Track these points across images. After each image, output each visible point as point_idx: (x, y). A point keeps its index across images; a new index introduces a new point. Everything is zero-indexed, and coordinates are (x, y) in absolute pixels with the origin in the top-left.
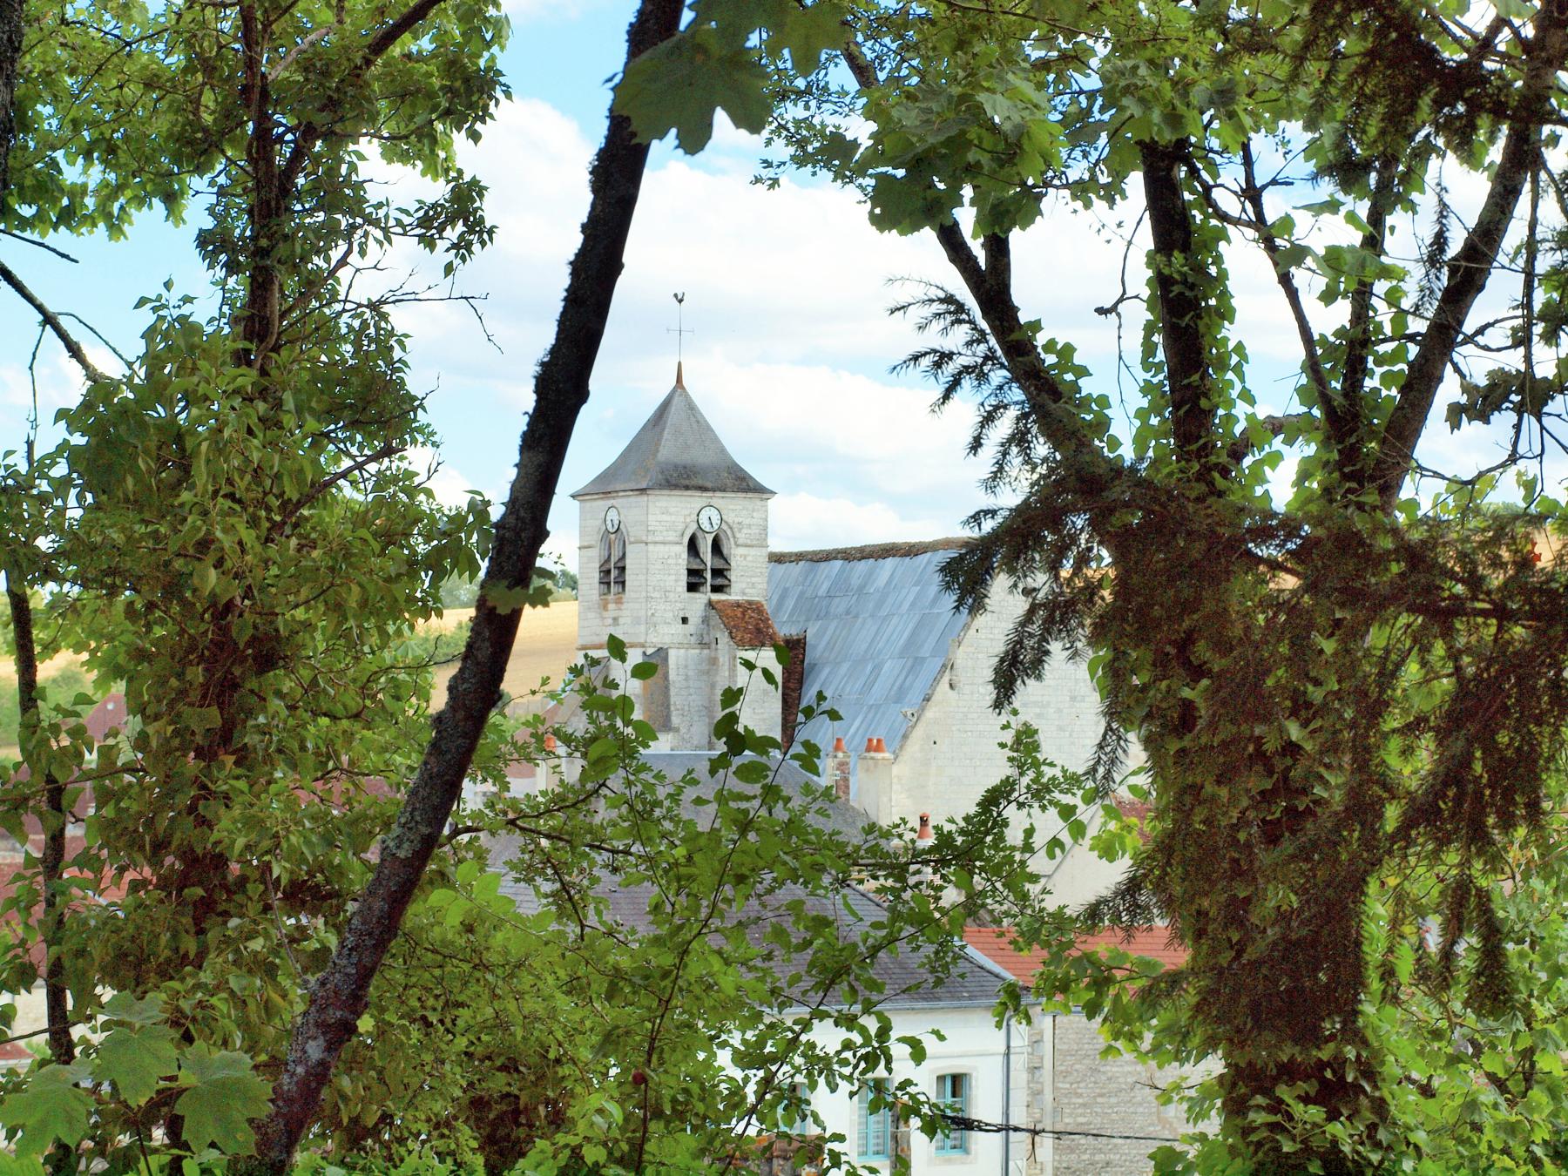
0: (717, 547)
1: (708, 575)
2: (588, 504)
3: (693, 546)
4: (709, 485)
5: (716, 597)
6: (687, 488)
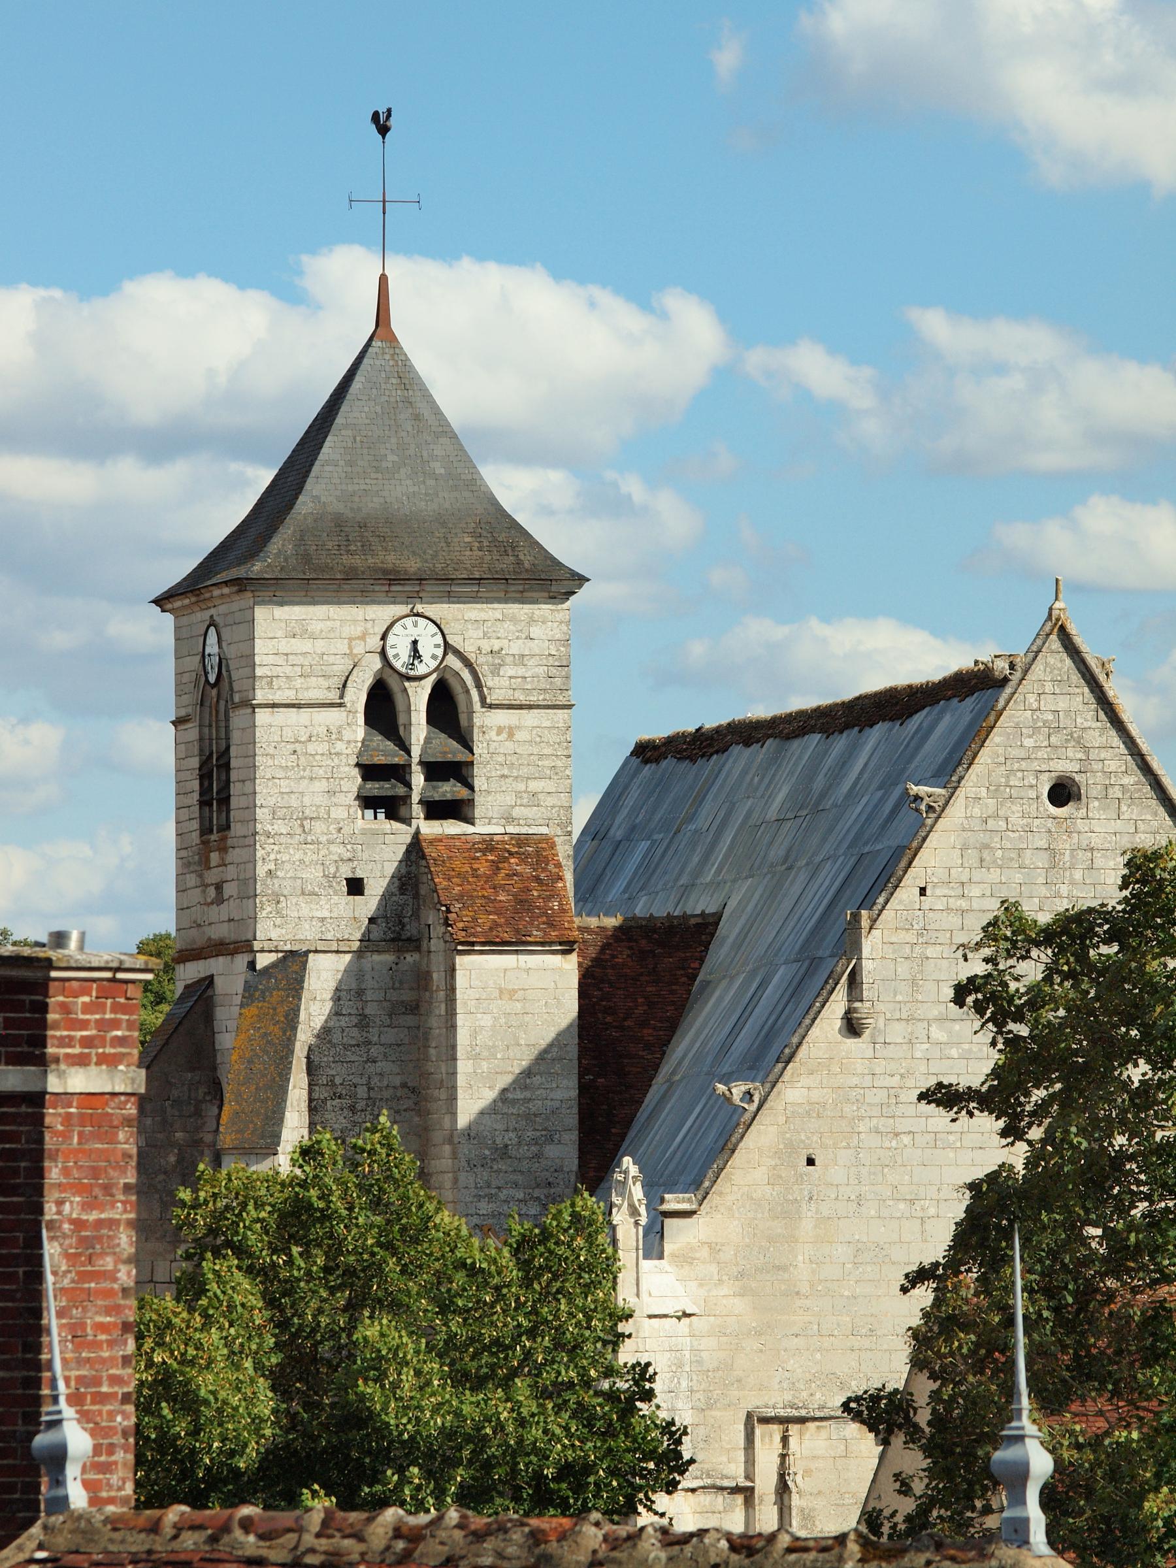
1: (418, 779)
2: (185, 620)
3: (382, 708)
4: (413, 565)
5: (430, 829)
6: (351, 575)
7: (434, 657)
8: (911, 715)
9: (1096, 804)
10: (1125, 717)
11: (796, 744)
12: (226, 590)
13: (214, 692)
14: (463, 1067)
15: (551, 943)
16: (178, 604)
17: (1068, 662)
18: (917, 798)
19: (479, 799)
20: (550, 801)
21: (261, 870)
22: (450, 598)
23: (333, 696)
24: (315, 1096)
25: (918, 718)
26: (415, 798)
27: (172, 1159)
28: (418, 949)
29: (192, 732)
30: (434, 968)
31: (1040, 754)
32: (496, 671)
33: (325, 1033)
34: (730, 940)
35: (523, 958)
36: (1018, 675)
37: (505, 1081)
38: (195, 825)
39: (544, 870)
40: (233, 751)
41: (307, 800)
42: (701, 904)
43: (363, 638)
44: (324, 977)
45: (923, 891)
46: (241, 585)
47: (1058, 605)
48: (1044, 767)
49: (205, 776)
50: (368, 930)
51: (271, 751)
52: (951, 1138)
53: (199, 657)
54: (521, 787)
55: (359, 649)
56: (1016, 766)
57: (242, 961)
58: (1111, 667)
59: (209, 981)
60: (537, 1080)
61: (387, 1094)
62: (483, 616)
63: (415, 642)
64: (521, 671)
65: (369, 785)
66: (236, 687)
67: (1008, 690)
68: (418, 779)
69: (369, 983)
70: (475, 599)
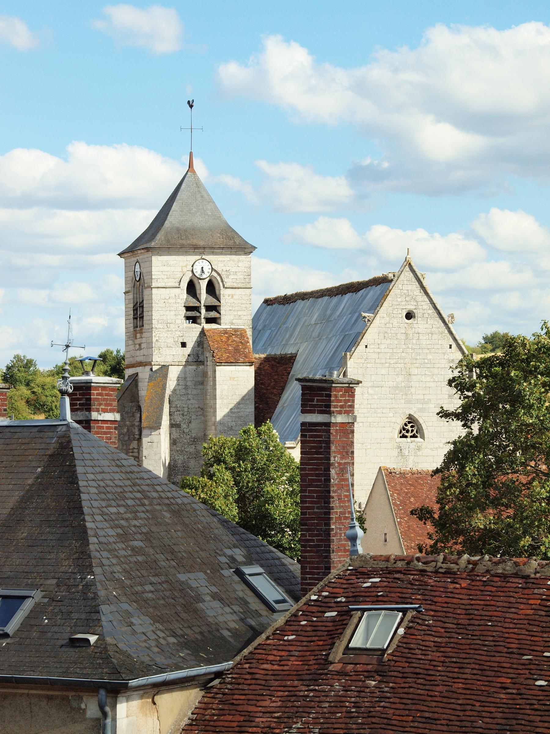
0: (211, 288)
1: (203, 311)
2: (128, 261)
3: (192, 288)
4: (202, 243)
5: (208, 326)
6: (182, 247)
7: (208, 272)
8: (359, 291)
9: (420, 319)
10: (429, 292)
11: (320, 300)
12: (143, 251)
13: (138, 283)
14: (218, 402)
15: (246, 363)
16: (126, 255)
17: (411, 274)
18: (364, 317)
19: (222, 317)
20: (245, 318)
21: (154, 340)
22: (213, 253)
23: (177, 285)
24: (171, 410)
25: (361, 292)
26: (202, 317)
27: (125, 430)
28: (203, 364)
29: (131, 296)
30: (209, 370)
31: (403, 304)
32: (228, 277)
33: (174, 391)
34: (301, 362)
35: (237, 367)
36: (396, 278)
37: (231, 406)
38: (132, 325)
39: (243, 340)
40: (145, 302)
41: (168, 317)
42: (290, 350)
43: (186, 266)
44: (174, 373)
45: (366, 346)
46: (148, 249)
47: (408, 257)
48: (404, 308)
49: (135, 310)
50: (188, 358)
51: (157, 302)
52: (375, 424)
53: (133, 272)
54: (236, 313)
55: (185, 270)
56: (395, 307)
57: (148, 368)
58: (425, 276)
59: (137, 374)
60: (242, 406)
61: (194, 410)
62: (224, 259)
63: (202, 268)
64: (235, 277)
65: (188, 313)
66: (146, 281)
67: (393, 283)
68: (203, 311)
69: (188, 375)
70: (221, 254)
